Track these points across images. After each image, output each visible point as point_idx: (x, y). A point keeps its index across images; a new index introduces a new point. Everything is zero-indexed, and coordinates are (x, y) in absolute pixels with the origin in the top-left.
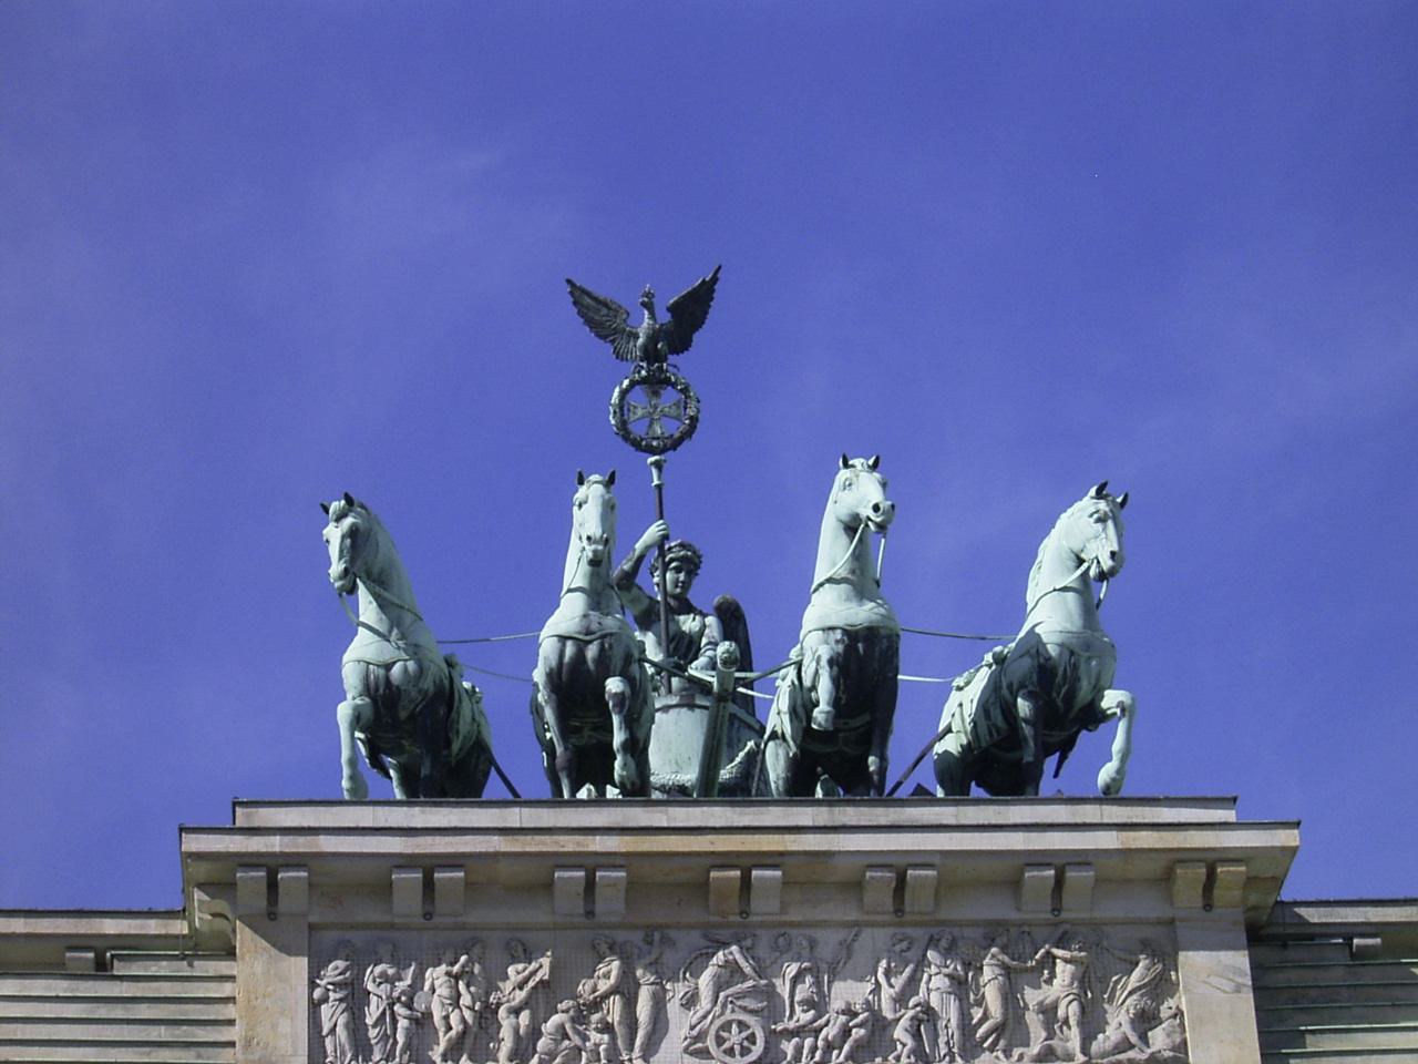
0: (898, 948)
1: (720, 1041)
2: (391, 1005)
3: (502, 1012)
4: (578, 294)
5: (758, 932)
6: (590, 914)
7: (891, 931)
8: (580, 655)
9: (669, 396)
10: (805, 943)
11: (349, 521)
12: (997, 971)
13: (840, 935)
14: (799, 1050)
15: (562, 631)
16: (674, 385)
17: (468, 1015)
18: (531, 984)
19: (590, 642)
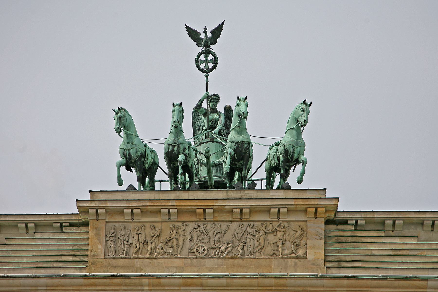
0: (240, 227)
1: (197, 250)
2: (124, 241)
3: (148, 243)
4: (188, 28)
5: (208, 223)
6: (169, 219)
7: (239, 223)
8: (173, 150)
9: (210, 57)
10: (219, 226)
11: (119, 114)
12: (264, 233)
13: (228, 224)
14: (215, 252)
15: (169, 143)
16: (212, 54)
17: (141, 244)
18: (155, 236)
19: (175, 146)
